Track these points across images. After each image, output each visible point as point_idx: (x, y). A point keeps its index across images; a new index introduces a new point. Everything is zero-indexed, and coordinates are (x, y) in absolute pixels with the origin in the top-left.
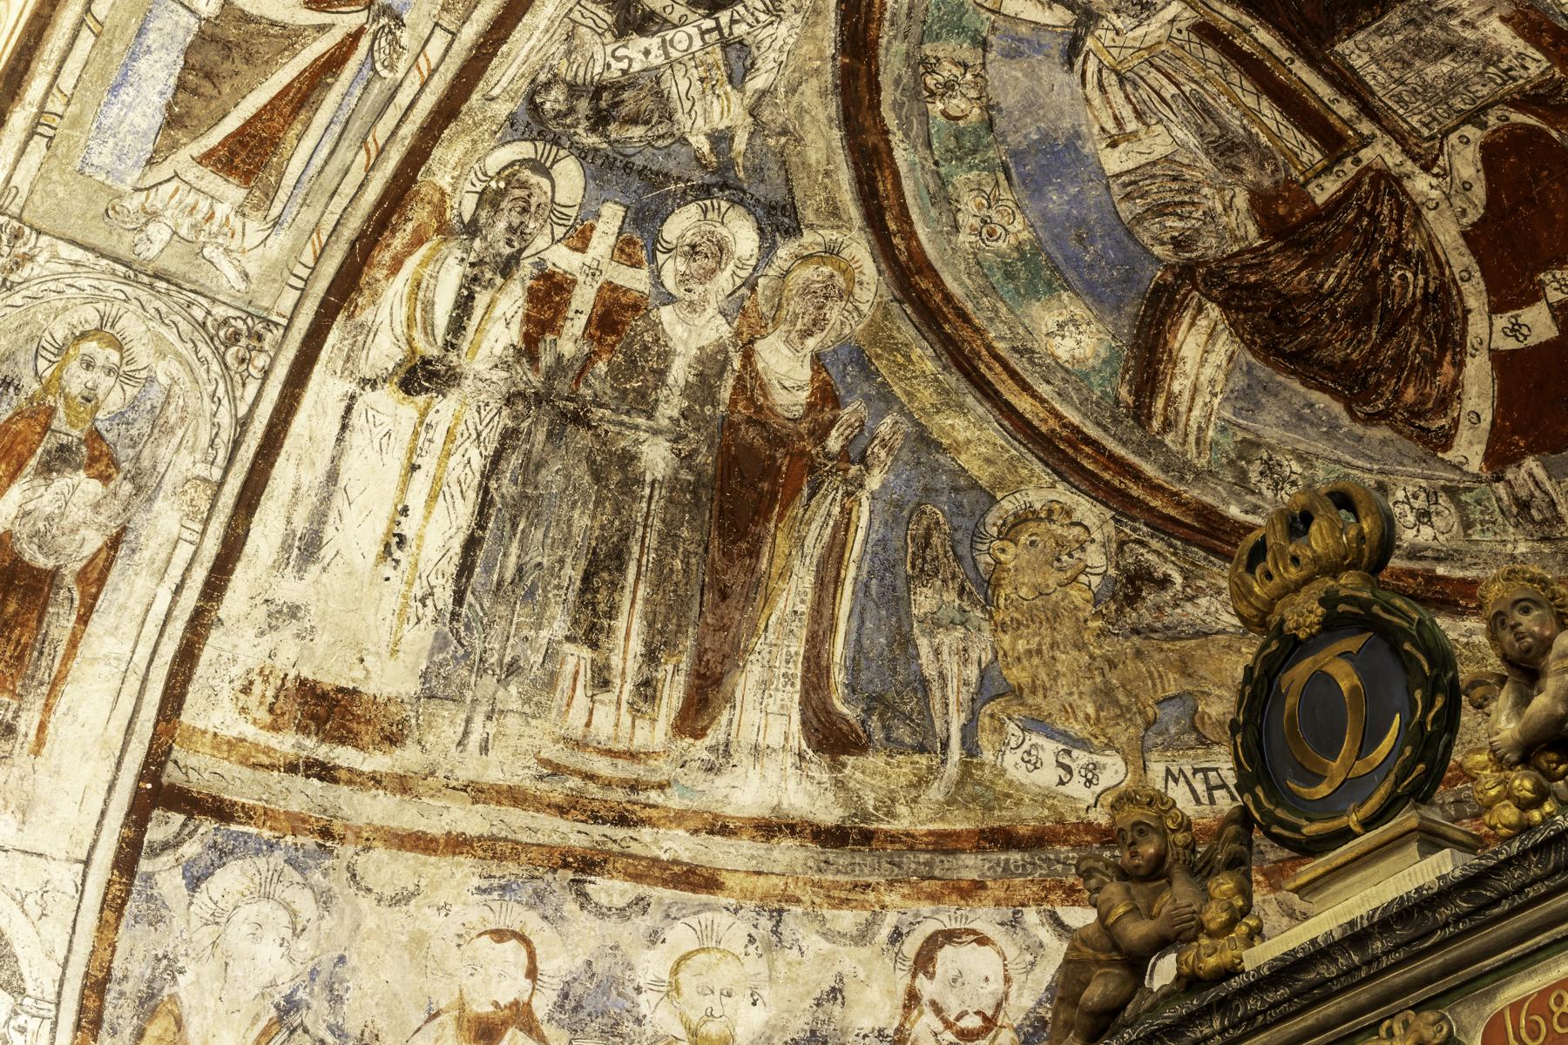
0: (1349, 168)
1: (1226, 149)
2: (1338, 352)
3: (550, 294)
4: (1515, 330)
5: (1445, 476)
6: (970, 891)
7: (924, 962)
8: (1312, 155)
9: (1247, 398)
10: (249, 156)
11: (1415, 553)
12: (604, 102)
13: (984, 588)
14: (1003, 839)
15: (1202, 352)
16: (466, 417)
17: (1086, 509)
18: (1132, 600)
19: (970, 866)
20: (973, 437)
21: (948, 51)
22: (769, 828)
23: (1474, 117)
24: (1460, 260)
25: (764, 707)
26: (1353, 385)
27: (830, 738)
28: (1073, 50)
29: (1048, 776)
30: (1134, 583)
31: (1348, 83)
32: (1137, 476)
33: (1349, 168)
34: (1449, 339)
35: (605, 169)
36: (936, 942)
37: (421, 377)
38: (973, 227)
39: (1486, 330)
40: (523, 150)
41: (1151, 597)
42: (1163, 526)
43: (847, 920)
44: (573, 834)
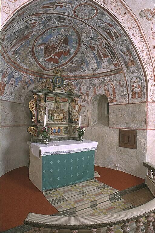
0: (57, 47)
1: (55, 42)
2: (46, 52)
3: (35, 23)
4: (53, 57)
5: (44, 59)
6: (11, 65)
7: (8, 68)
8: (57, 45)
9: (41, 50)
10: (44, 7)
11: (39, 61)
12: (50, 19)
13: (25, 49)
14: (14, 63)
15: (43, 47)
16: (25, 24)
17: (31, 49)
18: (27, 54)
19: (12, 64)
20: (33, 42)
21: (57, 30)
22: (8, 57)
23: (62, 50)
24: (54, 53)
25: (13, 50)
26: (45, 53)
27: (13, 53)
28: (59, 35)
29: (18, 60)
30: (29, 53)
31: (61, 45)
32: (34, 49)
33: (57, 47)
34: (50, 55)
35: (45, 21)
36: (9, 67)
37: (27, 21)
38: (45, 35)
39: (52, 56)
40: (45, 17)
41: (28, 54)
42: (32, 52)
43: (7, 64)
44: (3, 52)
